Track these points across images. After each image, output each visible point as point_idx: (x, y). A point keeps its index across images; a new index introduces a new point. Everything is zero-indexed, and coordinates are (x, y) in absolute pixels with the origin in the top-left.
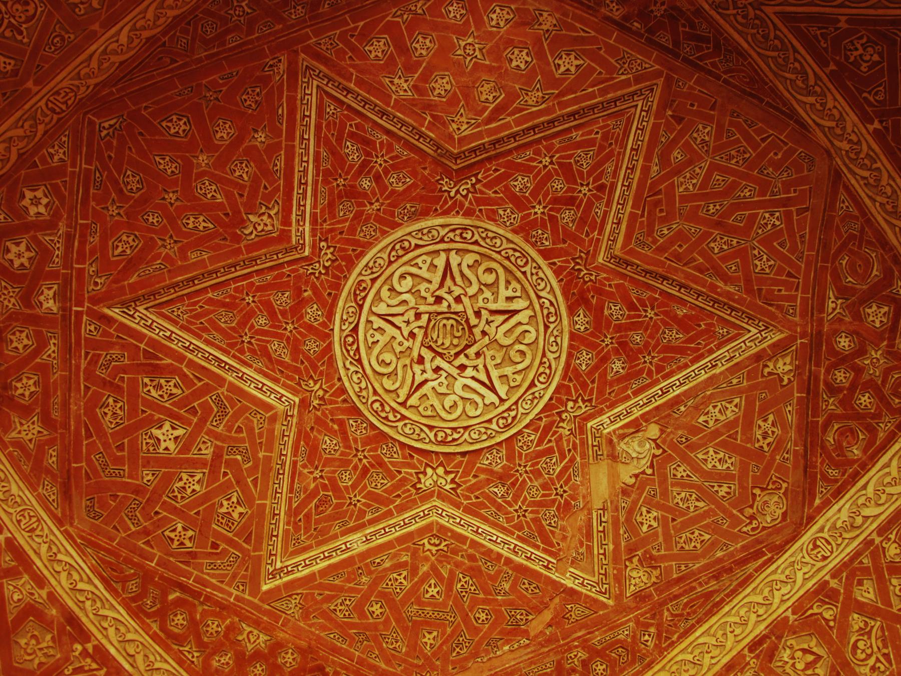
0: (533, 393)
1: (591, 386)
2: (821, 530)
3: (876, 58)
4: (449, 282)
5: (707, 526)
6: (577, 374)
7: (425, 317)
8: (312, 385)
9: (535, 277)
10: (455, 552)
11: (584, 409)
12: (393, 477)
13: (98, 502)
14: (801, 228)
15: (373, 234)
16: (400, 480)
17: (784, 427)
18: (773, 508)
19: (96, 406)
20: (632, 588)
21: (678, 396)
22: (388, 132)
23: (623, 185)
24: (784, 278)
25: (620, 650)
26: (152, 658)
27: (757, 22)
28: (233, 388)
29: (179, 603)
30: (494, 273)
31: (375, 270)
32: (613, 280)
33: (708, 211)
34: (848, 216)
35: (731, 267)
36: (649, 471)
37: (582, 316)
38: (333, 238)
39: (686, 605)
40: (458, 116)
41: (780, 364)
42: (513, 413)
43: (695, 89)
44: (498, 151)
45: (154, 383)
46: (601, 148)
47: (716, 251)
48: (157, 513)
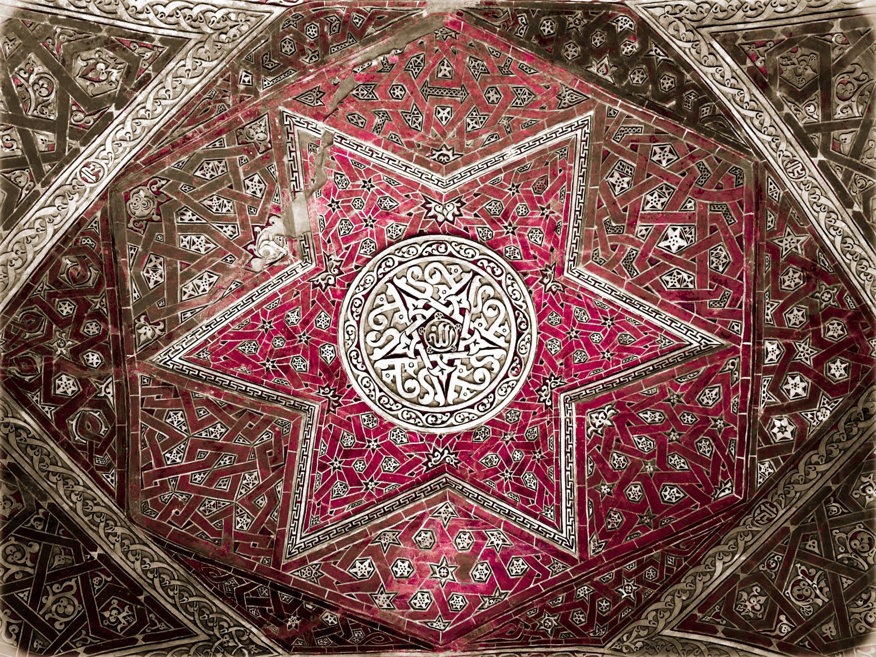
0: (365, 289)
2: (92, 190)
3: (106, 614)
4: (444, 379)
6: (327, 307)
9: (372, 388)
14: (145, 453)
16: (475, 209)
19: (733, 264)
21: (238, 298)
22: (503, 499)
23: (305, 471)
24: (156, 409)
25: (270, 67)
26: (693, 51)
27: (211, 625)
28: (620, 282)
29: (667, 99)
30: (406, 388)
31: (506, 385)
34: (107, 468)
35: (204, 413)
36: (257, 229)
37: (328, 358)
38: (541, 409)
39: (212, 112)
42: (381, 271)
44: (412, 491)
46: (326, 500)
47: (219, 426)
48: (683, 174)
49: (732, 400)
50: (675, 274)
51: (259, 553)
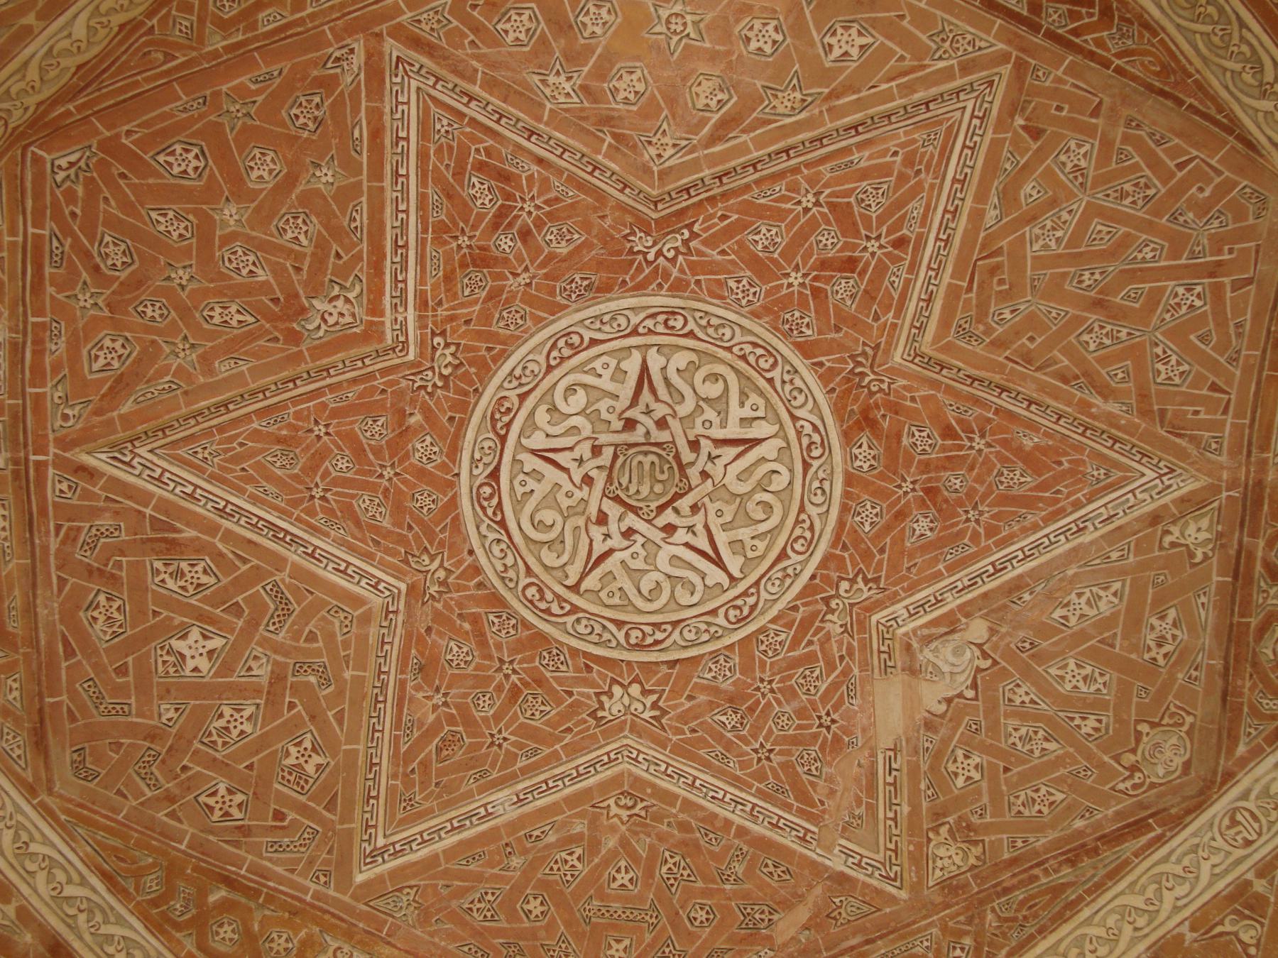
1: (878, 557)
2: (1245, 796)
4: (646, 396)
5: (1059, 781)
6: (857, 539)
8: (427, 562)
9: (788, 387)
10: (658, 818)
11: (866, 592)
12: (559, 702)
13: (91, 755)
15: (519, 321)
16: (571, 706)
17: (1192, 629)
18: (1169, 754)
19: (78, 608)
20: (938, 873)
21: (1020, 576)
22: (540, 161)
23: (937, 239)
24: (1205, 392)
28: (298, 572)
29: (226, 906)
30: (721, 382)
31: (524, 380)
32: (918, 390)
33: (1080, 282)
35: (1115, 374)
36: (970, 694)
37: (865, 446)
38: (454, 331)
39: (1022, 903)
40: (658, 135)
41: (1191, 529)
43: (1065, 83)
44: (726, 188)
45: (171, 569)
46: (902, 178)
47: (1092, 347)
48: (185, 768)
49: (62, 344)
50: (191, 588)
51: (1054, 93)
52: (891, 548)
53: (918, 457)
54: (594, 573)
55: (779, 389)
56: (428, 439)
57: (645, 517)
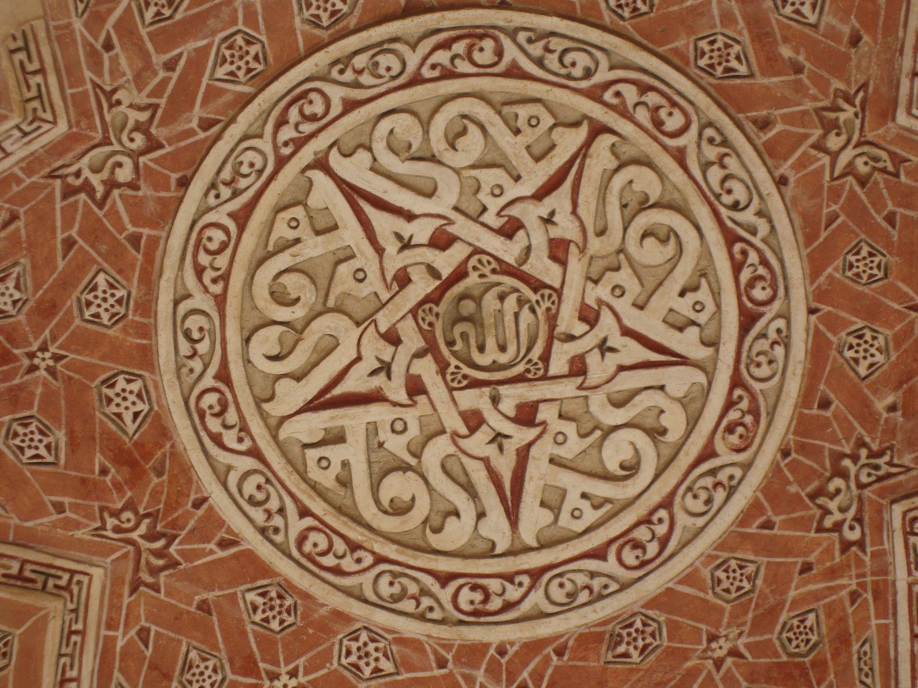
0: (236, 194)
1: (74, 233)
4: (505, 466)
6: (115, 255)
7: (559, 365)
8: (859, 162)
9: (274, 505)
15: (721, 574)
30: (385, 503)
31: (708, 481)
32: (54, 525)
37: (128, 417)
38: (828, 551)
42: (287, 133)
52: (53, 249)
53: (34, 411)
54: (566, 157)
55: (288, 501)
56: (863, 371)
57: (485, 258)
